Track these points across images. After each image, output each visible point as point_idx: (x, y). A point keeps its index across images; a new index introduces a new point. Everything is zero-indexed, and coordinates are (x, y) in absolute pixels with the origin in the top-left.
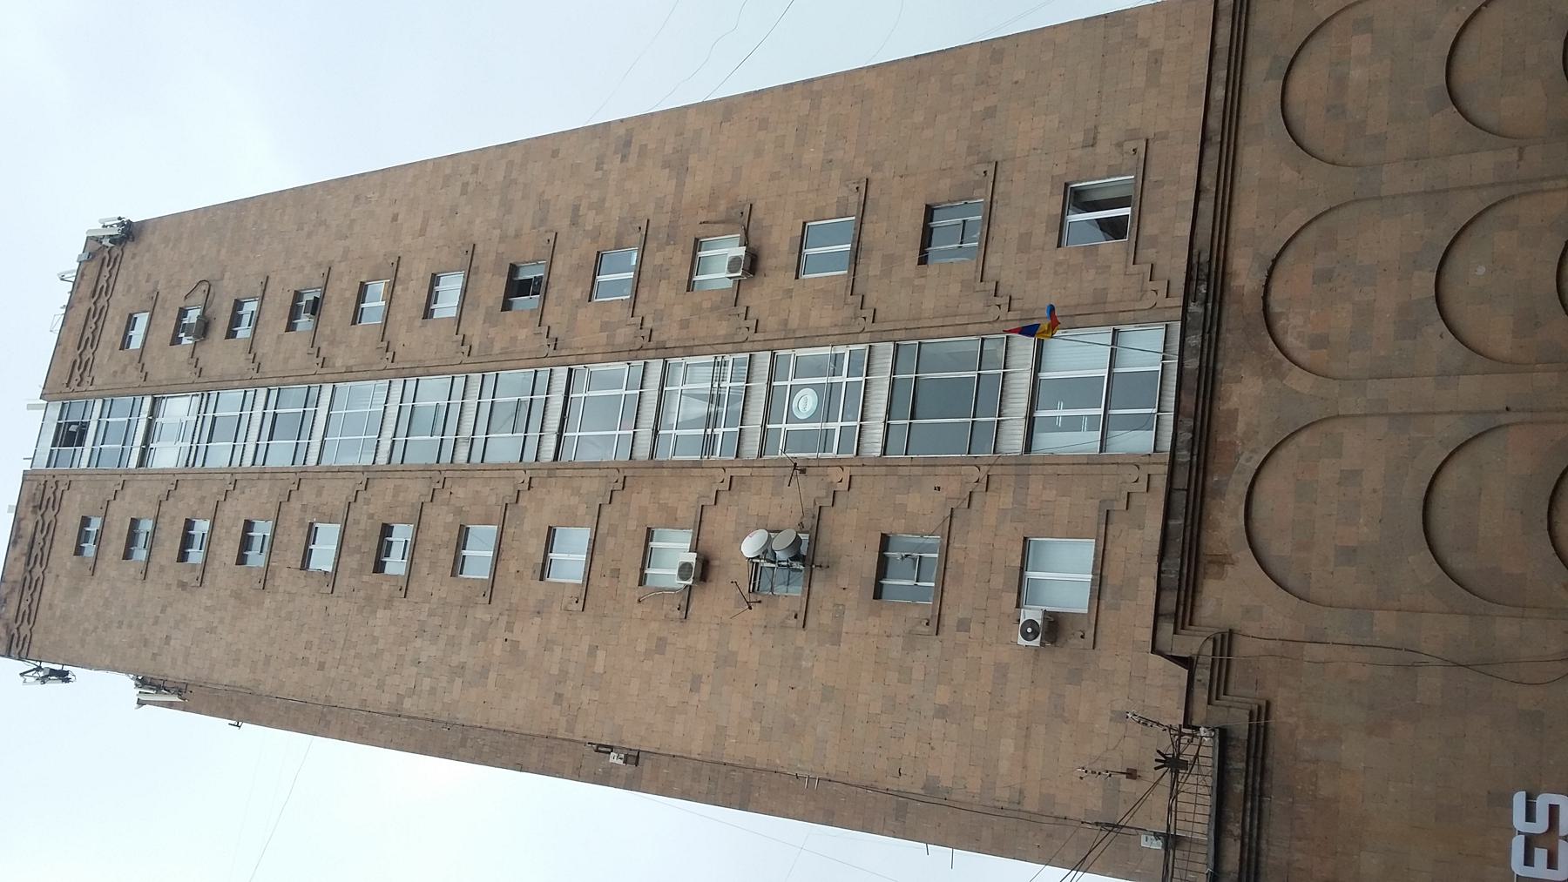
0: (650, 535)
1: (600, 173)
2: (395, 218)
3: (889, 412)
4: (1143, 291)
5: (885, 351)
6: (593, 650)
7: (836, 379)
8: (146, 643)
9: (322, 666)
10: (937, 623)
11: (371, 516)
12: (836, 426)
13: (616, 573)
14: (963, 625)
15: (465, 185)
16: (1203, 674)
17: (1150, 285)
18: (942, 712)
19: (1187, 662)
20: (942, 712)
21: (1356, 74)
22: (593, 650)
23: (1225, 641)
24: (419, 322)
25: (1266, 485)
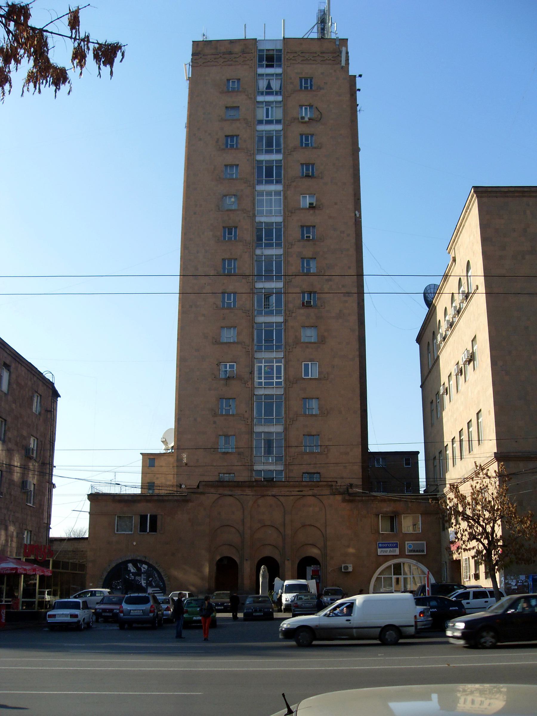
0: (235, 327)
1: (340, 286)
2: (336, 204)
3: (266, 395)
4: (290, 457)
5: (281, 391)
6: (204, 315)
7: (275, 378)
8: (199, 129)
9: (195, 213)
10: (215, 415)
11: (240, 221)
12: (263, 381)
13: (224, 319)
14: (215, 422)
15: (342, 232)
16: (196, 491)
17: (292, 458)
18: (195, 420)
19: (198, 487)
20: (195, 420)
21: (311, 509)
22: (204, 315)
23: (203, 493)
24: (300, 224)
25: (231, 499)
